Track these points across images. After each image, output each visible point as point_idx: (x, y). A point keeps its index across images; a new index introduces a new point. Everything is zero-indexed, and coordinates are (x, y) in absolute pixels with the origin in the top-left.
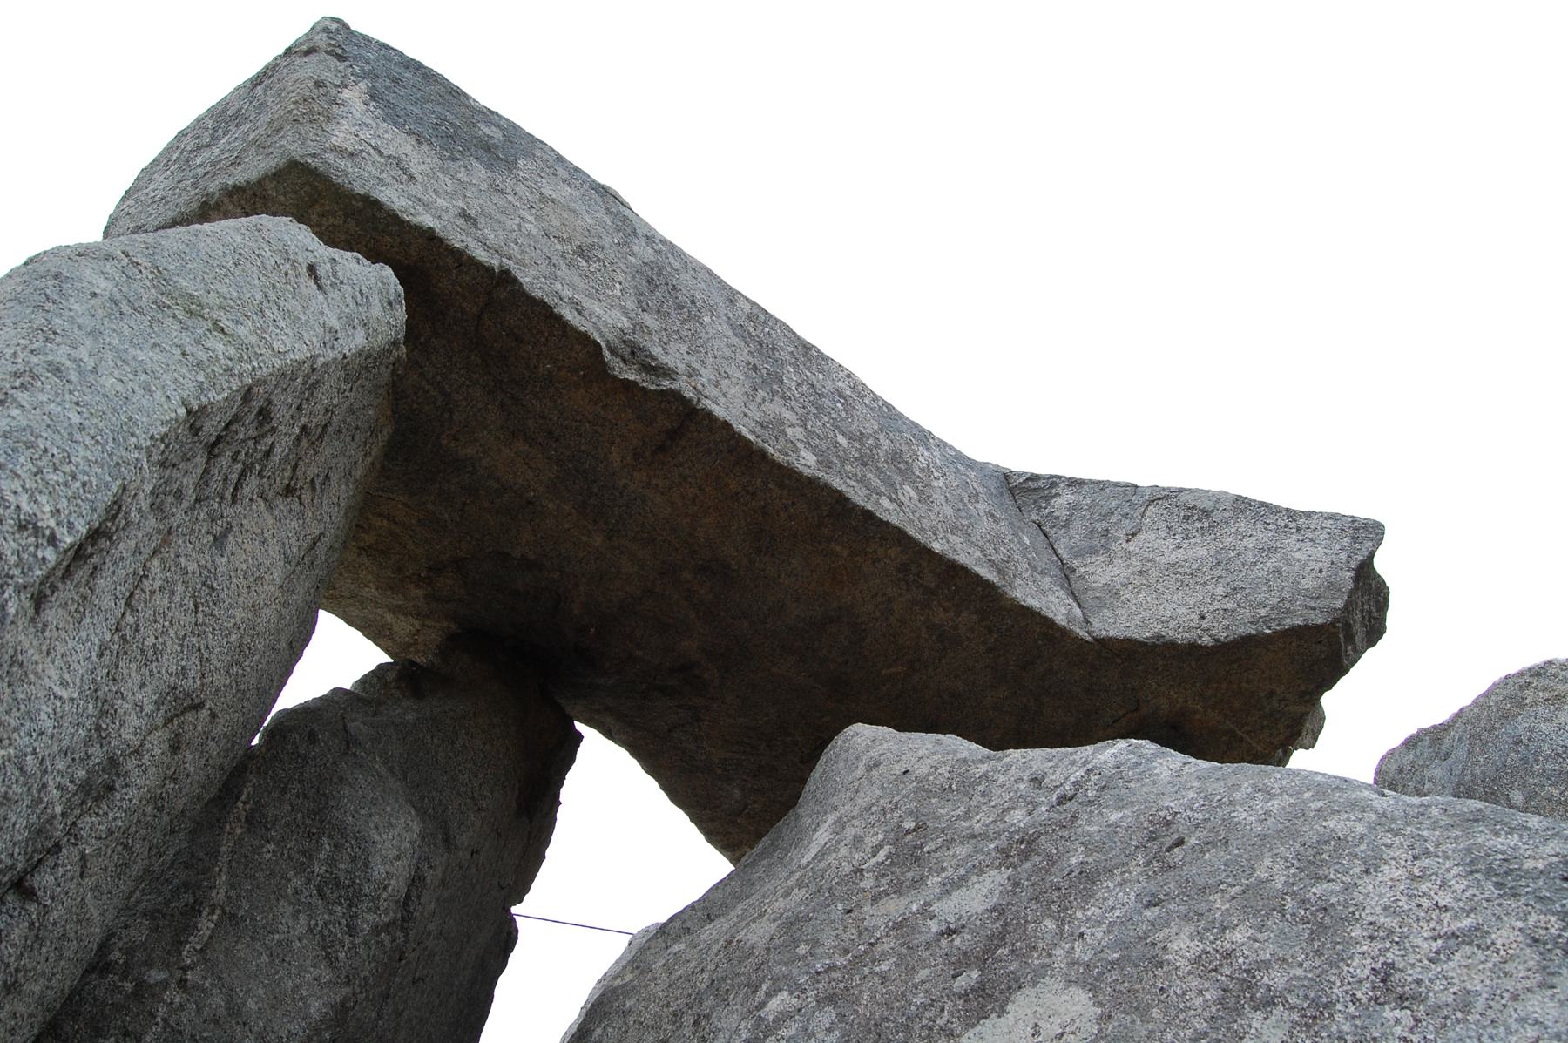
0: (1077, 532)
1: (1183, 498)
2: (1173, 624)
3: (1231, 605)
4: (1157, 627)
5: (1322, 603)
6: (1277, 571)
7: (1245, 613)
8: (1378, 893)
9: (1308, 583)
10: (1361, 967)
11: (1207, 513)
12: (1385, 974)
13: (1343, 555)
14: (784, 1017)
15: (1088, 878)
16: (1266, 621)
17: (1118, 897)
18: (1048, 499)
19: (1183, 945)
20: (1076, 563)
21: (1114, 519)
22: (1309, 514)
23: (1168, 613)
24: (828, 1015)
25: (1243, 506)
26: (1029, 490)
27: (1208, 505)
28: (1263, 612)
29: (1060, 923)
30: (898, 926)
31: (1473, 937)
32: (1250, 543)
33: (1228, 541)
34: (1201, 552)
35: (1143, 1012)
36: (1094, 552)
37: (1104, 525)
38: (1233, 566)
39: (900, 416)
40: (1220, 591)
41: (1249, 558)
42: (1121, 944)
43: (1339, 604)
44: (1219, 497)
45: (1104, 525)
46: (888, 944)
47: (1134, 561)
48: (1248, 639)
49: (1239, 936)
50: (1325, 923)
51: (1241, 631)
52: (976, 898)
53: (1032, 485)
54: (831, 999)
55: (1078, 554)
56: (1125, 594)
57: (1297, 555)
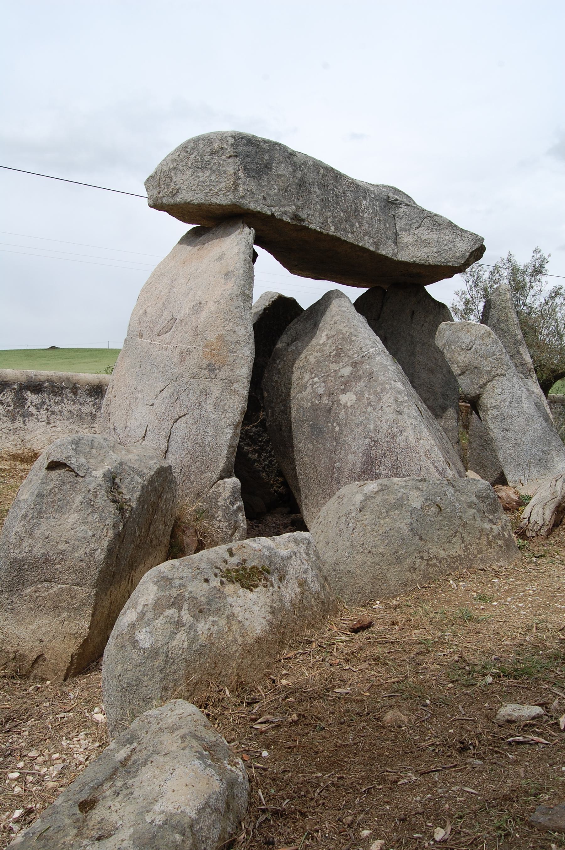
0: (403, 221)
1: (435, 218)
2: (419, 258)
3: (436, 255)
4: (415, 259)
5: (459, 261)
6: (451, 249)
7: (439, 259)
8: (386, 397)
9: (457, 254)
10: (380, 405)
11: (440, 225)
12: (382, 407)
13: (469, 248)
14: (317, 382)
15: (361, 377)
16: (443, 262)
17: (362, 384)
18: (398, 208)
19: (366, 395)
20: (400, 233)
21: (414, 221)
22: (466, 231)
23: (419, 255)
24: (323, 384)
25: (450, 224)
26: (394, 204)
27: (440, 222)
28: (443, 260)
29: (356, 384)
30: (335, 371)
31: (390, 406)
32: (447, 238)
33: (442, 235)
34: (434, 237)
35: (360, 401)
36: (406, 231)
37: (411, 222)
38: (441, 244)
39: (359, 190)
40: (435, 250)
41: (445, 243)
42: (360, 391)
43: (463, 262)
44: (444, 220)
45: (411, 222)
46: (333, 374)
47: (415, 237)
48: (437, 266)
49: (372, 397)
50: (380, 399)
51: (436, 263)
52: (347, 371)
53: (395, 202)
54: (324, 382)
55: (401, 230)
56: (410, 247)
57: (458, 245)
